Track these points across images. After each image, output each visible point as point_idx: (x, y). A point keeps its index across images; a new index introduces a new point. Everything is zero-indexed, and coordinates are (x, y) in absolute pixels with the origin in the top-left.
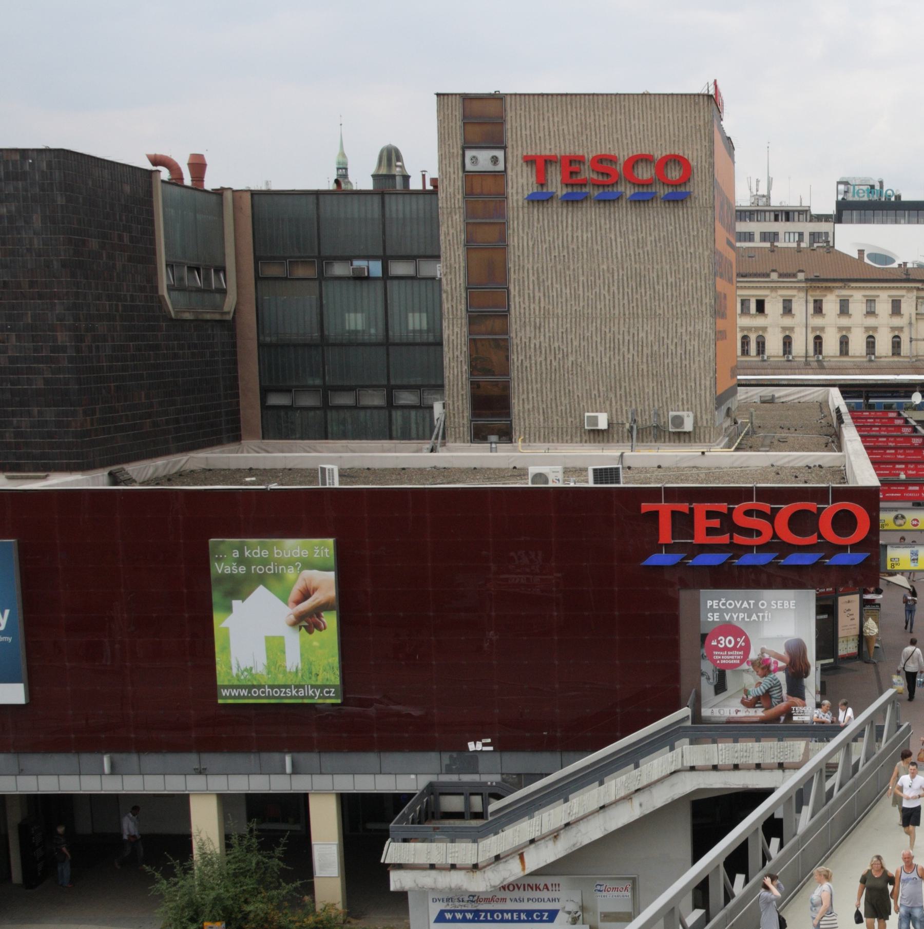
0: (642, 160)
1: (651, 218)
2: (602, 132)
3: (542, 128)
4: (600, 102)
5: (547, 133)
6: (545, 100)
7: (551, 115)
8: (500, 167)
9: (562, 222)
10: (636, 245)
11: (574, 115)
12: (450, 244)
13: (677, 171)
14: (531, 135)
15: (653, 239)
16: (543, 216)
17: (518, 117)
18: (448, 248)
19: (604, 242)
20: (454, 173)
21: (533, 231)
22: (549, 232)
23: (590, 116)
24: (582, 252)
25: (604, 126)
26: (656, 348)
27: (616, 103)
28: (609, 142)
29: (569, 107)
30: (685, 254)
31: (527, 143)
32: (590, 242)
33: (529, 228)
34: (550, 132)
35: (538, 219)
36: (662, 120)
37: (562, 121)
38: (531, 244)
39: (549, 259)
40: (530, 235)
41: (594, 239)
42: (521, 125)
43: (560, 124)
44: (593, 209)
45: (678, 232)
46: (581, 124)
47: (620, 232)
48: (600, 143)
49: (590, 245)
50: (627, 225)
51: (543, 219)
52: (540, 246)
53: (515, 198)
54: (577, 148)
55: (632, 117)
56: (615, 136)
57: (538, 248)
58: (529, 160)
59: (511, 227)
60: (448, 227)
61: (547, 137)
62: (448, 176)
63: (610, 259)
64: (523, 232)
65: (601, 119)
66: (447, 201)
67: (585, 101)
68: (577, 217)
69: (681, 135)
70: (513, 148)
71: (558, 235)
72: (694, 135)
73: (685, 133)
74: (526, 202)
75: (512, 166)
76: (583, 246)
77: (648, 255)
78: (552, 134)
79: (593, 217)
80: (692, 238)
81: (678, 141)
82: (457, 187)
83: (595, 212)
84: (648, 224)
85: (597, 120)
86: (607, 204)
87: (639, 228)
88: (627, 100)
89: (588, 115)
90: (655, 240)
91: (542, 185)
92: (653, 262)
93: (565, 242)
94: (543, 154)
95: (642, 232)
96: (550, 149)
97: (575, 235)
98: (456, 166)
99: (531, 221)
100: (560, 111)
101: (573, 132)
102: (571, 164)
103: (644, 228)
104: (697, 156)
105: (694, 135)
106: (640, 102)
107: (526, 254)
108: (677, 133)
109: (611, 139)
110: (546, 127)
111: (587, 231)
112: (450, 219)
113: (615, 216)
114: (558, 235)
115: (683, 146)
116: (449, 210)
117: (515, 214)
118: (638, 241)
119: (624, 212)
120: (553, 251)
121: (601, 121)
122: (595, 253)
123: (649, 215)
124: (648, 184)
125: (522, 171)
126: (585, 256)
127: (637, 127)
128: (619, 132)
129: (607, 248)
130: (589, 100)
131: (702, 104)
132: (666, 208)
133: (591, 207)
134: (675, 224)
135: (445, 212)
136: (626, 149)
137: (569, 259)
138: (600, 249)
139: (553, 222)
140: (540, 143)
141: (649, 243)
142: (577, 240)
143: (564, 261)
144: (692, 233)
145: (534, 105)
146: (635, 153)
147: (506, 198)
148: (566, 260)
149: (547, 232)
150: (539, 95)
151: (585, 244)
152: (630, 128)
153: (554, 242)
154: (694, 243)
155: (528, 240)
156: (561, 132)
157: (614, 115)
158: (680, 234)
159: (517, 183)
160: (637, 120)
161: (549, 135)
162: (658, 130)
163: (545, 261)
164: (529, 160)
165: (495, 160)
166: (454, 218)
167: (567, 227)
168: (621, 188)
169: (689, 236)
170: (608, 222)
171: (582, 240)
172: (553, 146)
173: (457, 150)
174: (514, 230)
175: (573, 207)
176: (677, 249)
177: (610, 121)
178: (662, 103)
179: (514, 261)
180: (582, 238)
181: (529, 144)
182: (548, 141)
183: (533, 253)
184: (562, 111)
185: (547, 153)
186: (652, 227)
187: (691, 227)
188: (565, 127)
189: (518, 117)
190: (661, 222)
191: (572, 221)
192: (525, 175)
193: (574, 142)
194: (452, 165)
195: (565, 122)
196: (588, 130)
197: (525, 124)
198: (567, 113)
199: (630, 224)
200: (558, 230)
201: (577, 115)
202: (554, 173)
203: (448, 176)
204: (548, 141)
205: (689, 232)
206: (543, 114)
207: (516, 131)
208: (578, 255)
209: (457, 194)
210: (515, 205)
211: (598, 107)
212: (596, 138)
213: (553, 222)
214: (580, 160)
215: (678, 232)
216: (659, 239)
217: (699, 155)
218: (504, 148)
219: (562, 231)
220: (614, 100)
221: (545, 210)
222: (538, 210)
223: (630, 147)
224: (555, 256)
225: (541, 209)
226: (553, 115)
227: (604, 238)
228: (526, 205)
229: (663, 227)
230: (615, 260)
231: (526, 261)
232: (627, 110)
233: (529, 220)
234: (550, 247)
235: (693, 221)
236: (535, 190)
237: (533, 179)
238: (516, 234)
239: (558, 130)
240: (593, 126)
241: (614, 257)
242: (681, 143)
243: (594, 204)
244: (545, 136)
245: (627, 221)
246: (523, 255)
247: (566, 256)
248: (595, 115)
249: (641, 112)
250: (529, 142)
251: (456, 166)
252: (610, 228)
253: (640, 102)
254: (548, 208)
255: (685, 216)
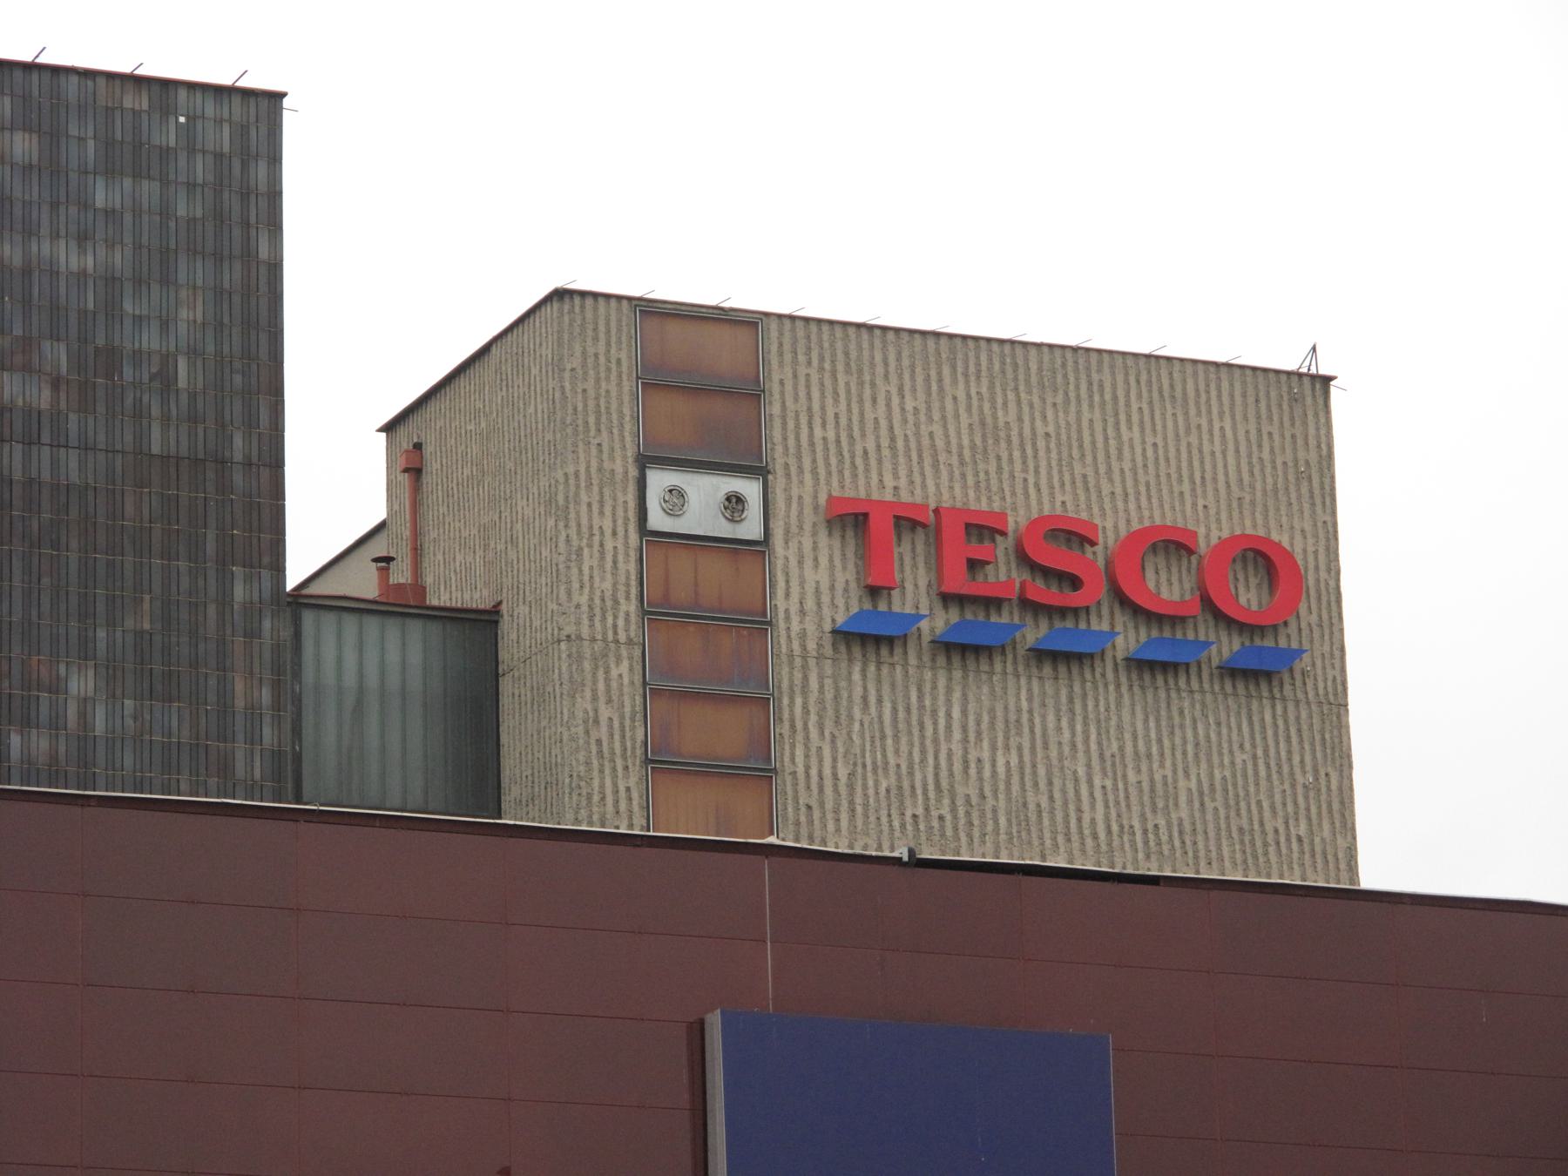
0: (1154, 549)
1: (1188, 722)
2: (1042, 453)
3: (870, 426)
4: (1034, 367)
5: (885, 443)
6: (877, 343)
7: (894, 391)
8: (751, 528)
9: (934, 712)
10: (1146, 798)
11: (961, 395)
12: (600, 753)
13: (1253, 590)
14: (838, 442)
15: (1193, 784)
16: (878, 691)
17: (802, 380)
18: (595, 763)
19: (1057, 782)
20: (614, 533)
21: (849, 734)
22: (896, 738)
23: (1005, 404)
24: (995, 811)
25: (1047, 434)
27: (1076, 370)
28: (1063, 485)
29: (946, 371)
30: (1282, 839)
31: (828, 465)
32: (1015, 780)
33: (837, 722)
34: (893, 439)
35: (865, 699)
36: (1205, 437)
37: (929, 409)
38: (843, 773)
39: (896, 824)
40: (839, 744)
41: (1028, 770)
42: (810, 409)
43: (923, 418)
44: (1023, 681)
45: (1263, 773)
46: (983, 423)
47: (1102, 756)
48: (1037, 485)
49: (1015, 788)
50: (1120, 739)
51: (880, 701)
52: (871, 783)
53: (795, 627)
54: (971, 493)
55: (1122, 417)
56: (1078, 469)
57: (865, 787)
59: (786, 716)
60: (595, 698)
61: (886, 452)
62: (596, 539)
63: (1075, 837)
64: (822, 733)
65: (1037, 415)
66: (591, 618)
67: (990, 360)
68: (979, 700)
69: (1259, 486)
70: (788, 476)
71: (923, 752)
72: (1292, 488)
73: (1270, 480)
74: (828, 639)
75: (787, 532)
76: (995, 792)
77: (1181, 833)
78: (900, 444)
79: (1025, 705)
80: (1300, 790)
81: (1253, 503)
82: (622, 579)
83: (1029, 690)
84: (1178, 741)
85: (1026, 418)
86: (1062, 669)
87: (1155, 750)
88: (1106, 370)
89: (1000, 401)
90: (1201, 794)
92: (1196, 857)
93: (944, 774)
94: (875, 496)
95: (1162, 765)
96: (896, 488)
97: (972, 757)
98: (620, 512)
99: (844, 703)
100: (920, 379)
101: (960, 447)
103: (1167, 752)
104: (1305, 551)
105: (1292, 488)
106: (1144, 377)
107: (829, 805)
108: (1246, 476)
109: (1067, 478)
110: (883, 423)
111: (1007, 748)
112: (601, 674)
113: (1085, 706)
114: (923, 752)
115: (1266, 517)
116: (598, 646)
117: (798, 676)
118: (1152, 790)
119: (1112, 698)
120: (908, 802)
121: (1038, 423)
122: (1033, 817)
123: (1181, 712)
125: (815, 548)
126: (1002, 821)
127: (1138, 450)
128: (1089, 459)
129: (1066, 803)
130: (1003, 356)
131: (1309, 400)
132: (1226, 696)
133: (1018, 676)
134: (1254, 746)
135: (587, 652)
136: (1109, 512)
137: (956, 829)
138: (1044, 804)
139: (908, 710)
140: (867, 470)
141: (1183, 799)
142: (980, 772)
143: (943, 835)
144: (1300, 779)
145: (847, 354)
146: (1136, 526)
147: (770, 623)
148: (949, 833)
149: (889, 741)
150: (859, 326)
151: (1002, 786)
152: (1120, 450)
153: (911, 774)
154: (1308, 809)
155: (835, 760)
156: (926, 442)
157: (1073, 408)
158: (1269, 777)
159: (802, 584)
160: (1136, 428)
161: (893, 447)
162: (1196, 464)
163: (885, 828)
165: (735, 503)
166: (614, 673)
167: (949, 727)
168: (1100, 625)
169: (1293, 786)
170: (1064, 723)
171: (994, 773)
172: (903, 482)
174: (793, 726)
175: (964, 668)
176: (1262, 824)
177: (1063, 423)
178: (1202, 387)
179: (797, 823)
180: (994, 765)
181: (834, 469)
182: (887, 465)
183: (851, 802)
184: (927, 379)
185: (889, 497)
186: (1190, 748)
187: (1296, 759)
188: (937, 429)
189: (802, 380)
190: (1213, 736)
191: (964, 712)
192: (824, 561)
193: (963, 475)
194: (608, 510)
195: (936, 416)
196: (1003, 445)
197: (823, 408)
198: (941, 389)
199: (1127, 736)
200: (922, 737)
201: (969, 397)
202: (908, 560)
203: (596, 539)
204: (887, 465)
205: (1292, 774)
206: (873, 385)
207: (797, 426)
208: (982, 815)
209: (622, 601)
210: (796, 646)
211: (1027, 381)
212: (1025, 470)
213: (908, 710)
214: (984, 529)
215: (1263, 773)
216: (1212, 786)
217: (1310, 549)
218: (759, 471)
219: (936, 741)
220: (1070, 364)
221: (885, 670)
222: (864, 671)
223: (1120, 505)
224: (915, 816)
225: (872, 668)
226: (901, 389)
227: (1056, 771)
228: (828, 651)
229: (1221, 754)
230: (1089, 842)
231: (831, 826)
232: (1108, 397)
233: (836, 698)
234: (900, 788)
235: (1301, 741)
236: (855, 609)
237: (847, 575)
238: (800, 737)
239: (917, 434)
240: (1015, 433)
241: (1087, 832)
242: (1259, 509)
243: (1028, 666)
244: (879, 447)
245: (1120, 727)
246: (822, 804)
247: (948, 817)
248: (1019, 402)
249: (1145, 406)
250: (833, 461)
251: (620, 512)
252: (1073, 746)
253: (1144, 377)
254: (893, 665)
255: (1280, 723)
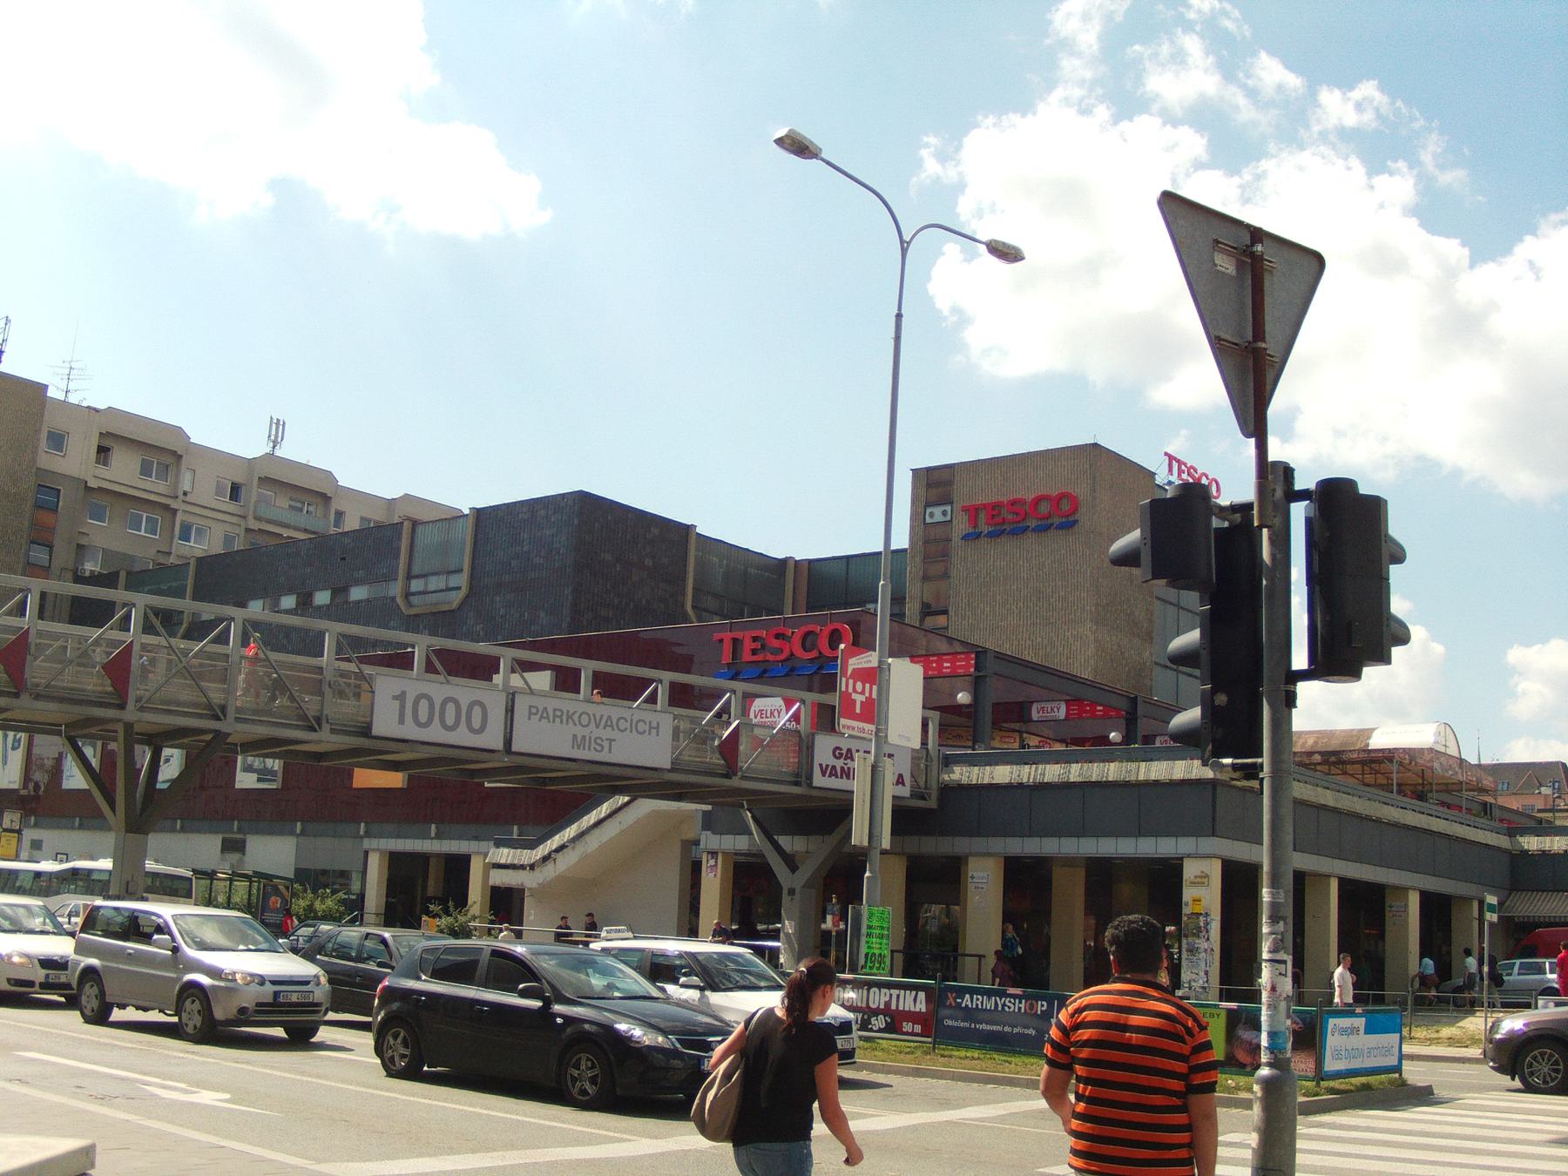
26: (1048, 650)
58: (965, 509)
91: (975, 527)
102: (993, 509)
124: (1049, 516)
164: (965, 509)
165: (944, 513)
173: (921, 510)
218: (952, 503)
